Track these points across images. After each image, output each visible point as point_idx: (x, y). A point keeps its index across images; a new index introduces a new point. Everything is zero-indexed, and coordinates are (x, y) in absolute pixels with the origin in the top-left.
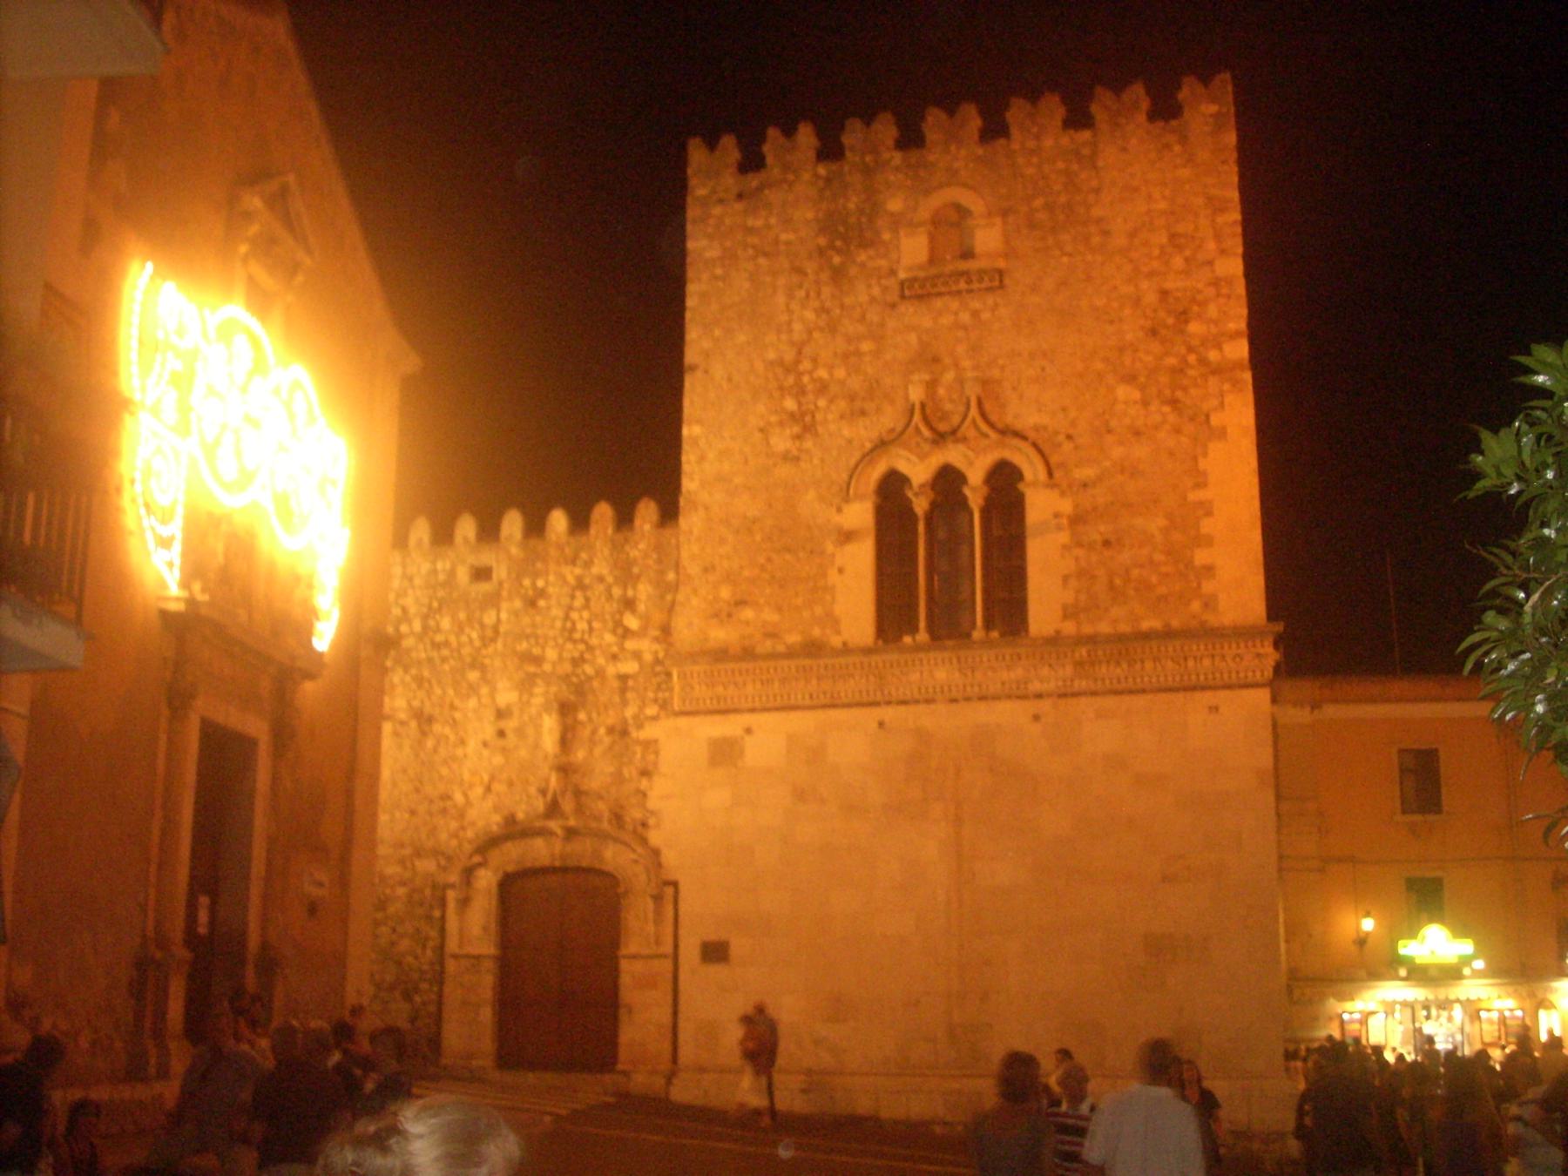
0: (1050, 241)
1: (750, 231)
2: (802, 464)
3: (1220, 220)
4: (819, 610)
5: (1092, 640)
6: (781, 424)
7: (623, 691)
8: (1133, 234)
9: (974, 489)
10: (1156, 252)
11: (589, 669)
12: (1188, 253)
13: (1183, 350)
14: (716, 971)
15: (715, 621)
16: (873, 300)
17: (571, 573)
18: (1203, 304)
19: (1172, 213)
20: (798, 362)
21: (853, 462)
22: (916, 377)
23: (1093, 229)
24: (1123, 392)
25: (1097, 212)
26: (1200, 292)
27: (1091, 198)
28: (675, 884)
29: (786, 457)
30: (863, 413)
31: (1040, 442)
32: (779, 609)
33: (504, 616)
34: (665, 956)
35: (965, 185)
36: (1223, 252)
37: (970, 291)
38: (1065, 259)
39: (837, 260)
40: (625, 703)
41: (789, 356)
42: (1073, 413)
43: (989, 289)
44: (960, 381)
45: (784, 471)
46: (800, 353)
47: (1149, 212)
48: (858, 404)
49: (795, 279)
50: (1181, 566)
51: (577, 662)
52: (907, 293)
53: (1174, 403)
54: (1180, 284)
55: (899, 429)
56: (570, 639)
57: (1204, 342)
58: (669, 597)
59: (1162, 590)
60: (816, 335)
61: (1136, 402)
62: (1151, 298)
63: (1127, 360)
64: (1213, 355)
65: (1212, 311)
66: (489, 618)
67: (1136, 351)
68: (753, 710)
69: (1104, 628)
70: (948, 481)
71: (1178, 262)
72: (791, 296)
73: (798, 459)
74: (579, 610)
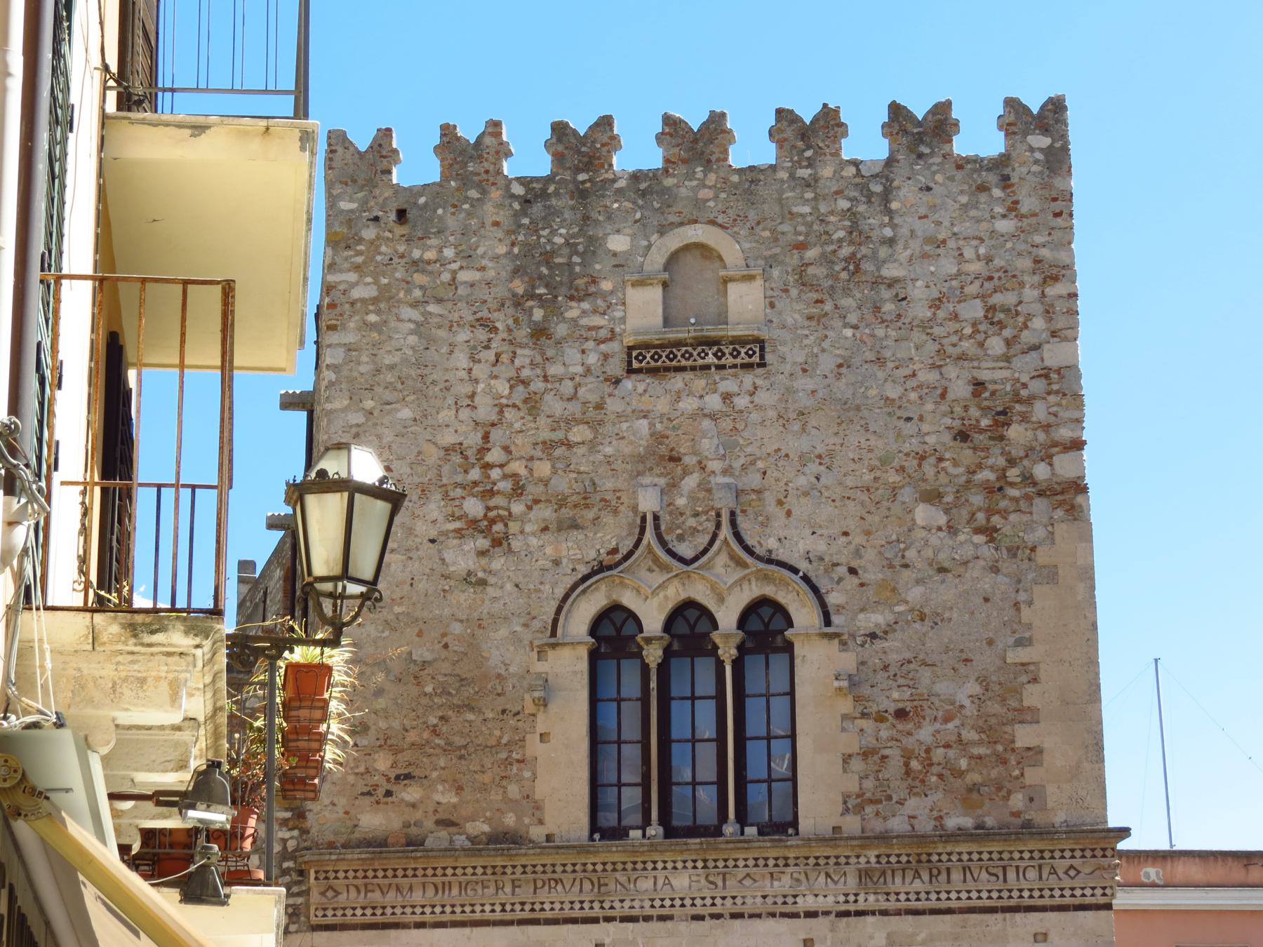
0: (828, 307)
1: (416, 265)
3: (1053, 290)
5: (884, 838)
6: (459, 533)
8: (936, 304)
9: (727, 636)
10: (968, 331)
12: (1007, 333)
13: (1001, 462)
16: (588, 371)
18: (1029, 401)
19: (991, 278)
20: (483, 451)
21: (560, 592)
22: (647, 480)
23: (886, 294)
24: (924, 514)
25: (890, 271)
26: (1025, 386)
27: (883, 252)
30: (575, 526)
31: (812, 575)
35: (712, 222)
36: (1054, 334)
37: (721, 367)
38: (849, 332)
39: (538, 314)
41: (474, 439)
42: (858, 539)
43: (744, 366)
44: (705, 487)
45: (463, 598)
46: (486, 437)
47: (959, 273)
48: (566, 513)
49: (482, 335)
52: (635, 365)
53: (989, 532)
54: (999, 374)
55: (624, 551)
57: (1029, 451)
60: (509, 414)
61: (940, 529)
62: (961, 390)
63: (929, 469)
64: (1041, 471)
65: (1040, 412)
67: (940, 460)
69: (898, 824)
70: (689, 624)
71: (996, 345)
72: (473, 359)
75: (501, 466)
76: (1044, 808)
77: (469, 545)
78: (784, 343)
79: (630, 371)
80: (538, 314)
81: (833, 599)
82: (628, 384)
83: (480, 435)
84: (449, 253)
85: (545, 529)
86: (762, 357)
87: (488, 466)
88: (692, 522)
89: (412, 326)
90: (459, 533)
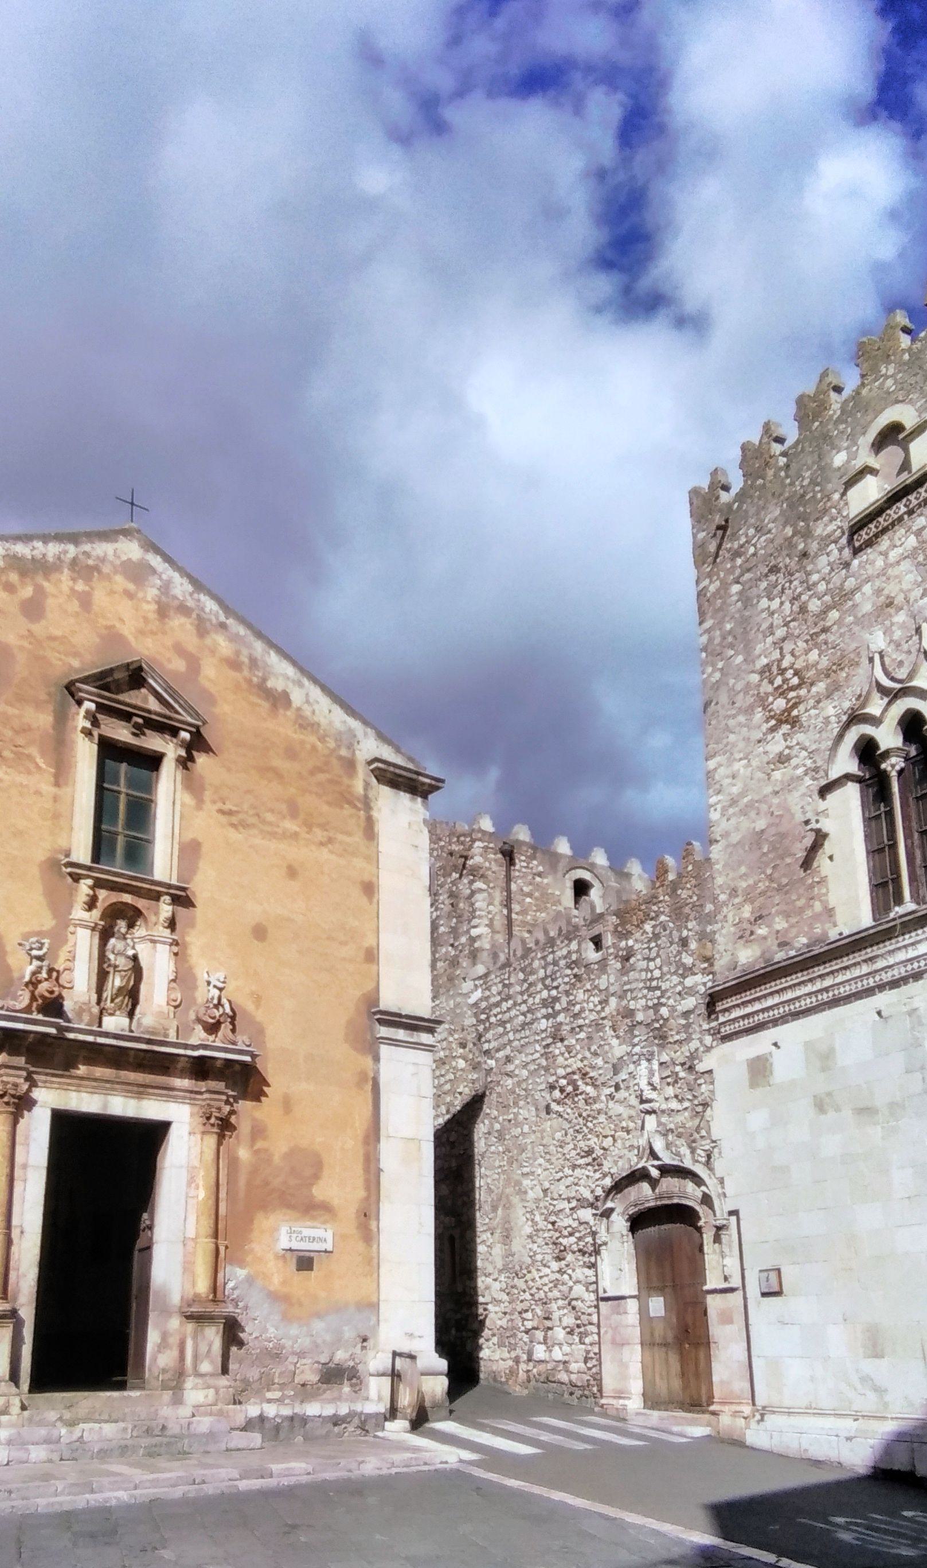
2: (794, 762)
4: (818, 906)
7: (687, 1026)
11: (664, 1011)
15: (742, 942)
17: (648, 927)
29: (782, 759)
30: (837, 689)
32: (787, 915)
40: (688, 1040)
51: (656, 1007)
56: (650, 989)
66: (603, 982)
73: (789, 758)
74: (653, 960)
75: (791, 668)
77: (778, 736)
83: (778, 651)
85: (818, 702)
87: (782, 671)
90: (772, 730)
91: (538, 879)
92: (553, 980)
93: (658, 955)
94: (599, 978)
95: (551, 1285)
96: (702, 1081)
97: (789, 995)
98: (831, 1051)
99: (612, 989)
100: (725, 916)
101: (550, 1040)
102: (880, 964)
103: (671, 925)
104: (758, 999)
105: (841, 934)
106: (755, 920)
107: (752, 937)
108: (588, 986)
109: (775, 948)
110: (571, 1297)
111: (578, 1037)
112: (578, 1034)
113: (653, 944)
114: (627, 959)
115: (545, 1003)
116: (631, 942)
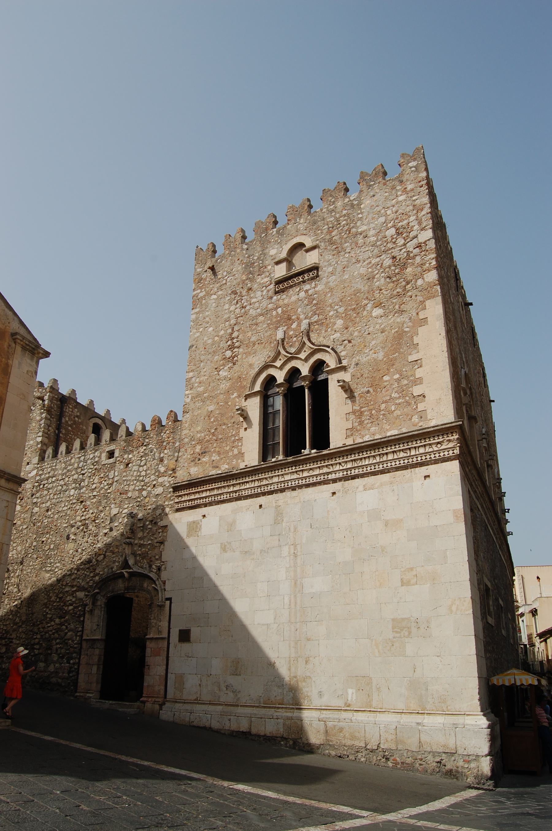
14: (185, 646)
17: (142, 449)
28: (170, 599)
31: (335, 347)
32: (219, 453)
33: (116, 474)
34: (163, 639)
37: (304, 282)
41: (230, 331)
43: (313, 279)
49: (233, 296)
50: (407, 398)
58: (176, 454)
59: (398, 412)
66: (111, 475)
68: (206, 505)
74: (143, 466)
76: (426, 419)
78: (325, 266)
79: (276, 293)
80: (249, 285)
81: (343, 354)
82: (275, 298)
84: (225, 274)
86: (318, 273)
88: (295, 339)
89: (214, 301)
91: (76, 419)
92: (82, 470)
93: (145, 464)
94: (110, 472)
95: (54, 631)
96: (160, 530)
97: (215, 492)
98: (234, 522)
99: (116, 479)
100: (186, 450)
101: (74, 501)
102: (265, 482)
103: (155, 450)
104: (199, 492)
105: (246, 466)
106: (202, 453)
107: (199, 462)
108: (102, 475)
109: (211, 469)
110: (66, 638)
111: (92, 501)
112: (93, 499)
113: (143, 458)
114: (127, 465)
115: (75, 481)
116: (130, 456)
